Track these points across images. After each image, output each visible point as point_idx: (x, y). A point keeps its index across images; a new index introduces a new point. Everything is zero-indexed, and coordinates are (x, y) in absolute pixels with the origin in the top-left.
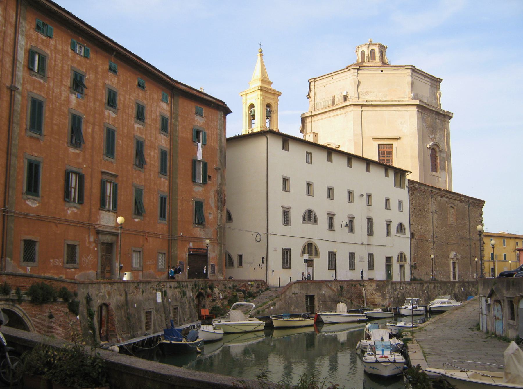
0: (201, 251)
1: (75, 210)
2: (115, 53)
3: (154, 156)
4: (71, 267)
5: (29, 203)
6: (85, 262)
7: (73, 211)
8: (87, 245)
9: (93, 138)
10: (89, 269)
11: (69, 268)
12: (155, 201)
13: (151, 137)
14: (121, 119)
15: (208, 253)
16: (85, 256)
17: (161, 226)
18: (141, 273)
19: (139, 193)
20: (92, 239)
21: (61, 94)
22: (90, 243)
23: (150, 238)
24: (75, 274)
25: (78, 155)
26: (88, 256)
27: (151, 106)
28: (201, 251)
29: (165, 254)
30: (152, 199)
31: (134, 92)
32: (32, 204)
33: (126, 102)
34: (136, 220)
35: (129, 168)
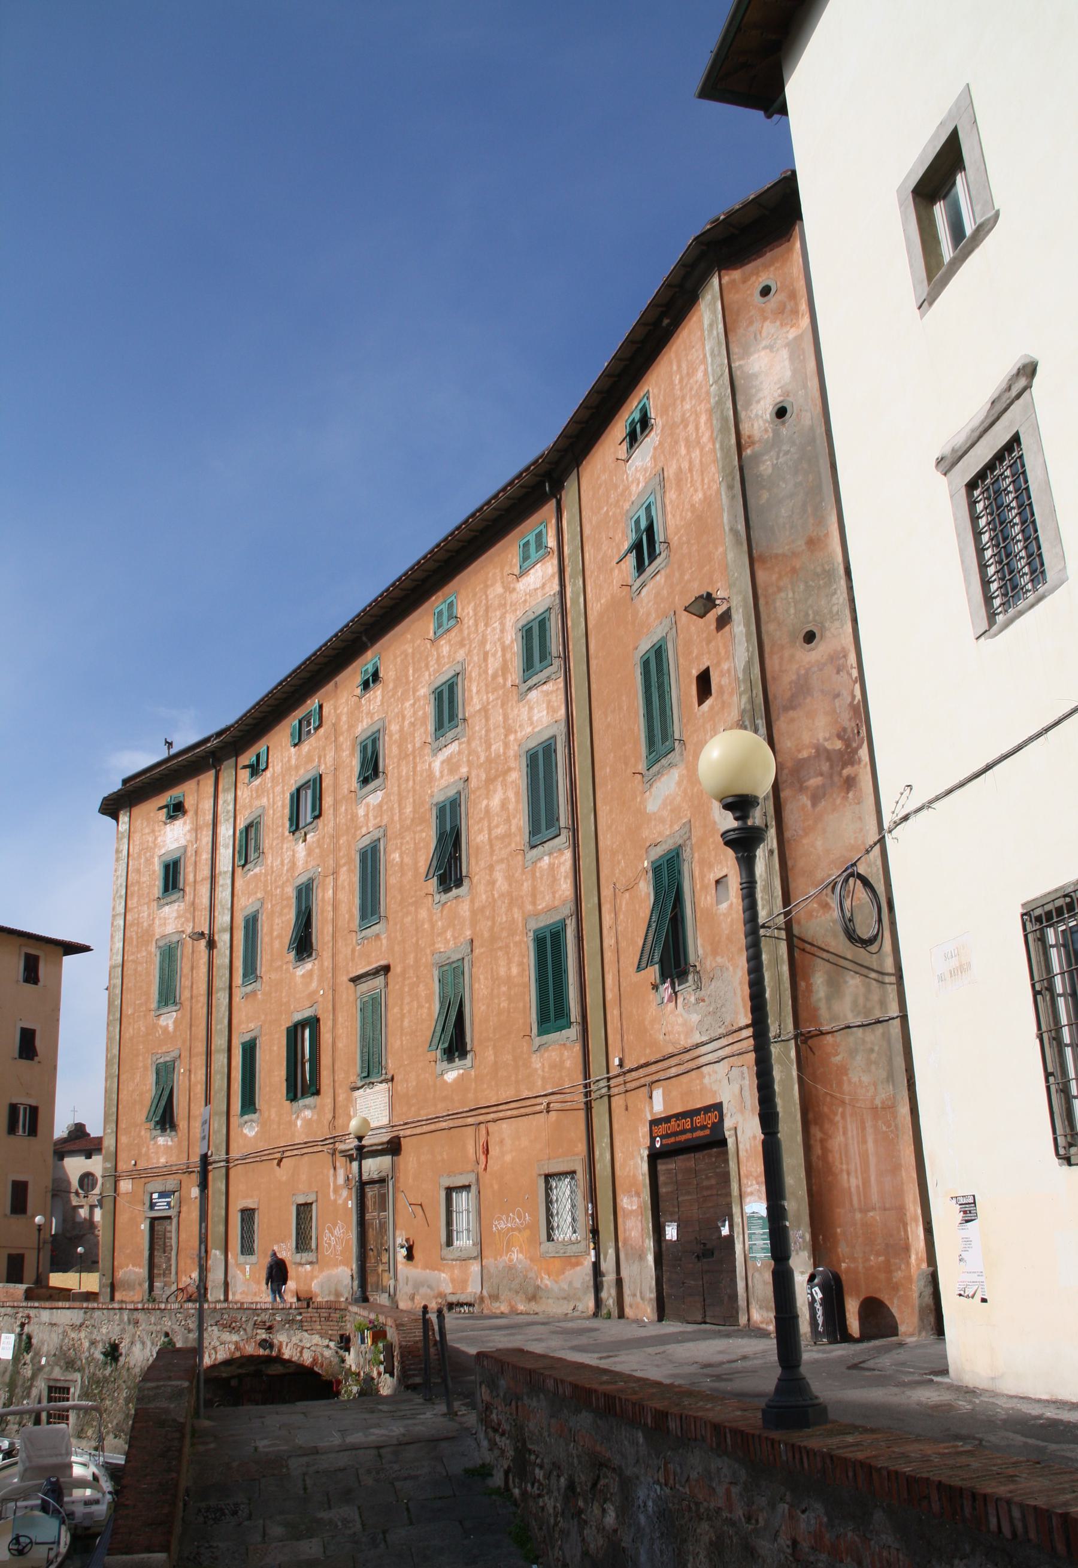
0: (698, 1120)
1: (308, 1113)
2: (364, 639)
3: (504, 805)
4: (303, 1261)
5: (246, 1131)
6: (329, 1244)
7: (305, 1119)
8: (332, 1197)
9: (335, 908)
10: (336, 1265)
11: (301, 1264)
12: (515, 971)
13: (489, 747)
14: (396, 789)
15: (728, 1123)
16: (329, 1229)
17: (556, 1058)
18: (475, 1268)
19: (453, 978)
20: (341, 1180)
21: (282, 864)
22: (336, 1191)
23: (504, 1125)
24: (312, 1279)
25: (310, 973)
26: (335, 1225)
27: (483, 643)
28: (698, 1120)
29: (572, 1173)
30: (502, 971)
31: (427, 666)
32: (249, 1131)
33: (406, 723)
34: (451, 1076)
35: (423, 914)
